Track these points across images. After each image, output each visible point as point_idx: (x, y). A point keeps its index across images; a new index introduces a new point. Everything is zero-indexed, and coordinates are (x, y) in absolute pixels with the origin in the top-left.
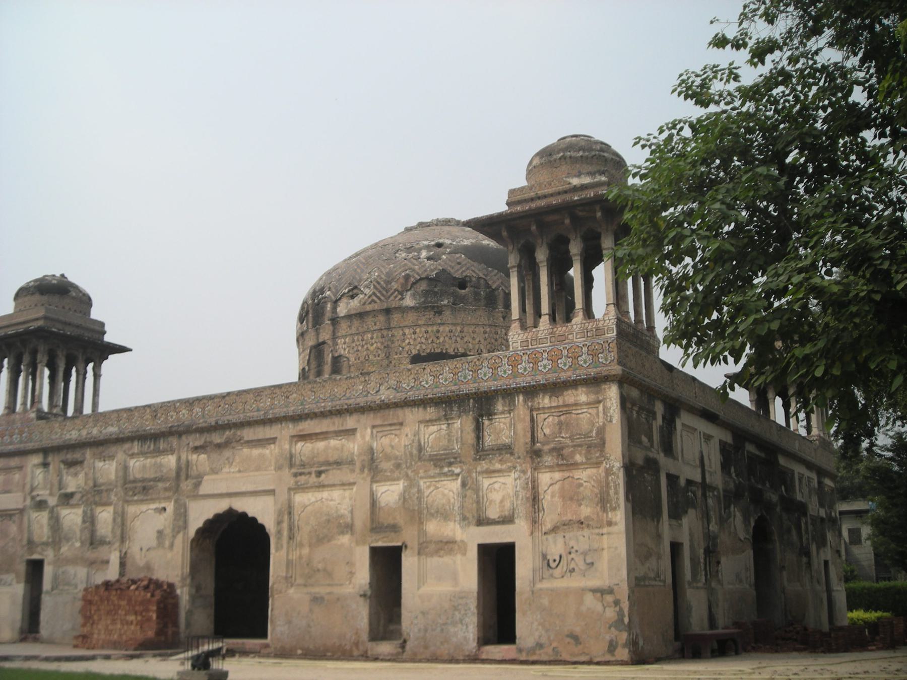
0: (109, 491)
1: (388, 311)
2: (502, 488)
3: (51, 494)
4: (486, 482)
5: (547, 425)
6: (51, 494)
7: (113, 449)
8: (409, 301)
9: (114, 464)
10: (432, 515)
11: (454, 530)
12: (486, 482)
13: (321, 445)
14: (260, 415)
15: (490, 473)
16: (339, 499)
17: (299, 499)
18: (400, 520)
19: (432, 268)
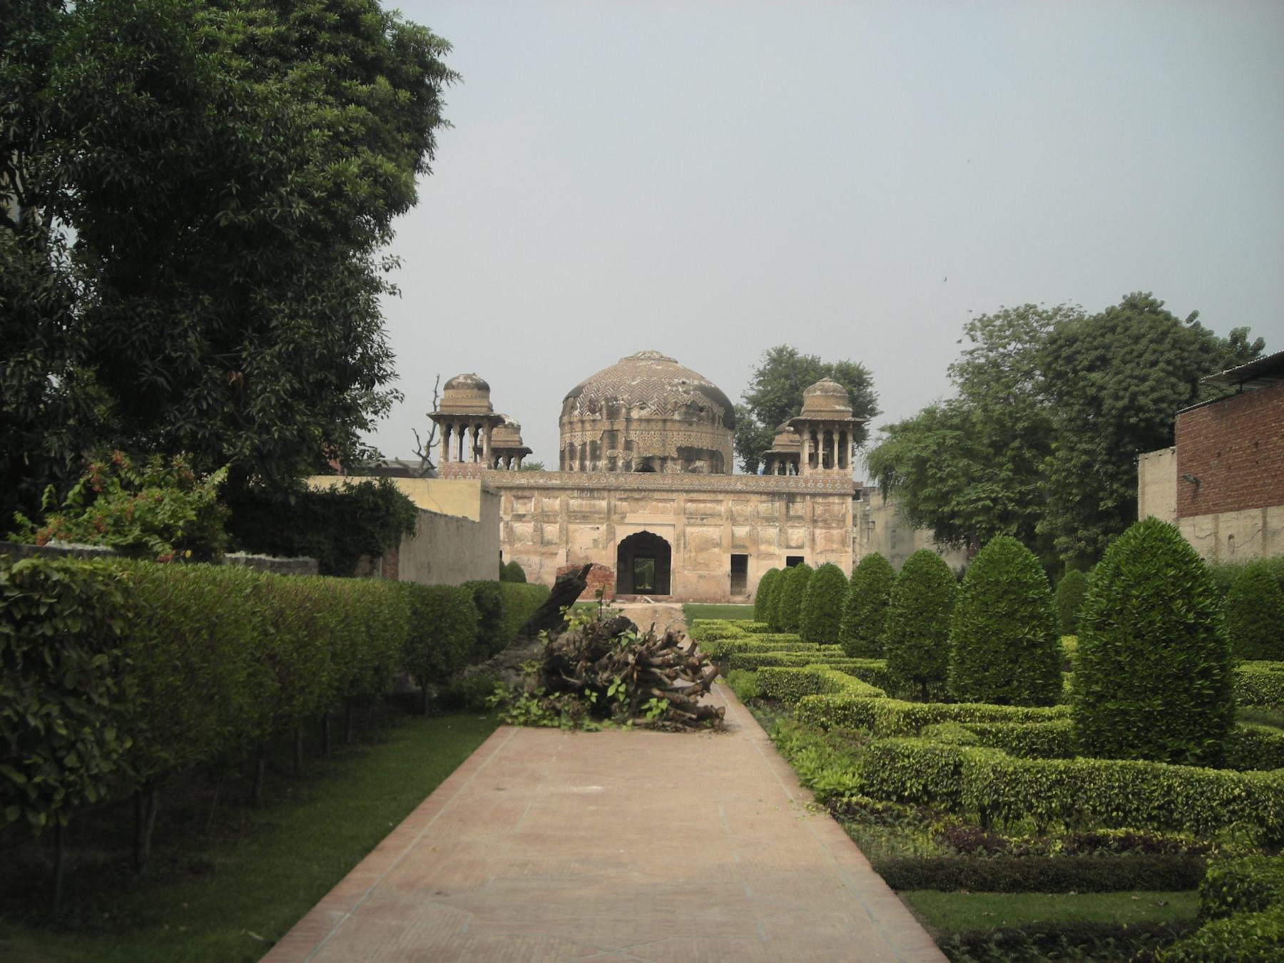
0: (555, 516)
1: (665, 421)
2: (798, 534)
3: (505, 513)
4: (790, 531)
5: (819, 510)
6: (505, 513)
7: (557, 493)
8: (677, 417)
9: (558, 501)
10: (763, 543)
11: (774, 549)
12: (790, 531)
13: (702, 505)
14: (667, 487)
15: (792, 527)
16: (711, 532)
17: (688, 529)
18: (747, 544)
19: (687, 399)
